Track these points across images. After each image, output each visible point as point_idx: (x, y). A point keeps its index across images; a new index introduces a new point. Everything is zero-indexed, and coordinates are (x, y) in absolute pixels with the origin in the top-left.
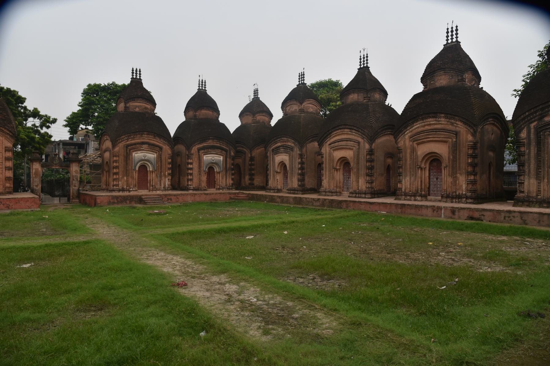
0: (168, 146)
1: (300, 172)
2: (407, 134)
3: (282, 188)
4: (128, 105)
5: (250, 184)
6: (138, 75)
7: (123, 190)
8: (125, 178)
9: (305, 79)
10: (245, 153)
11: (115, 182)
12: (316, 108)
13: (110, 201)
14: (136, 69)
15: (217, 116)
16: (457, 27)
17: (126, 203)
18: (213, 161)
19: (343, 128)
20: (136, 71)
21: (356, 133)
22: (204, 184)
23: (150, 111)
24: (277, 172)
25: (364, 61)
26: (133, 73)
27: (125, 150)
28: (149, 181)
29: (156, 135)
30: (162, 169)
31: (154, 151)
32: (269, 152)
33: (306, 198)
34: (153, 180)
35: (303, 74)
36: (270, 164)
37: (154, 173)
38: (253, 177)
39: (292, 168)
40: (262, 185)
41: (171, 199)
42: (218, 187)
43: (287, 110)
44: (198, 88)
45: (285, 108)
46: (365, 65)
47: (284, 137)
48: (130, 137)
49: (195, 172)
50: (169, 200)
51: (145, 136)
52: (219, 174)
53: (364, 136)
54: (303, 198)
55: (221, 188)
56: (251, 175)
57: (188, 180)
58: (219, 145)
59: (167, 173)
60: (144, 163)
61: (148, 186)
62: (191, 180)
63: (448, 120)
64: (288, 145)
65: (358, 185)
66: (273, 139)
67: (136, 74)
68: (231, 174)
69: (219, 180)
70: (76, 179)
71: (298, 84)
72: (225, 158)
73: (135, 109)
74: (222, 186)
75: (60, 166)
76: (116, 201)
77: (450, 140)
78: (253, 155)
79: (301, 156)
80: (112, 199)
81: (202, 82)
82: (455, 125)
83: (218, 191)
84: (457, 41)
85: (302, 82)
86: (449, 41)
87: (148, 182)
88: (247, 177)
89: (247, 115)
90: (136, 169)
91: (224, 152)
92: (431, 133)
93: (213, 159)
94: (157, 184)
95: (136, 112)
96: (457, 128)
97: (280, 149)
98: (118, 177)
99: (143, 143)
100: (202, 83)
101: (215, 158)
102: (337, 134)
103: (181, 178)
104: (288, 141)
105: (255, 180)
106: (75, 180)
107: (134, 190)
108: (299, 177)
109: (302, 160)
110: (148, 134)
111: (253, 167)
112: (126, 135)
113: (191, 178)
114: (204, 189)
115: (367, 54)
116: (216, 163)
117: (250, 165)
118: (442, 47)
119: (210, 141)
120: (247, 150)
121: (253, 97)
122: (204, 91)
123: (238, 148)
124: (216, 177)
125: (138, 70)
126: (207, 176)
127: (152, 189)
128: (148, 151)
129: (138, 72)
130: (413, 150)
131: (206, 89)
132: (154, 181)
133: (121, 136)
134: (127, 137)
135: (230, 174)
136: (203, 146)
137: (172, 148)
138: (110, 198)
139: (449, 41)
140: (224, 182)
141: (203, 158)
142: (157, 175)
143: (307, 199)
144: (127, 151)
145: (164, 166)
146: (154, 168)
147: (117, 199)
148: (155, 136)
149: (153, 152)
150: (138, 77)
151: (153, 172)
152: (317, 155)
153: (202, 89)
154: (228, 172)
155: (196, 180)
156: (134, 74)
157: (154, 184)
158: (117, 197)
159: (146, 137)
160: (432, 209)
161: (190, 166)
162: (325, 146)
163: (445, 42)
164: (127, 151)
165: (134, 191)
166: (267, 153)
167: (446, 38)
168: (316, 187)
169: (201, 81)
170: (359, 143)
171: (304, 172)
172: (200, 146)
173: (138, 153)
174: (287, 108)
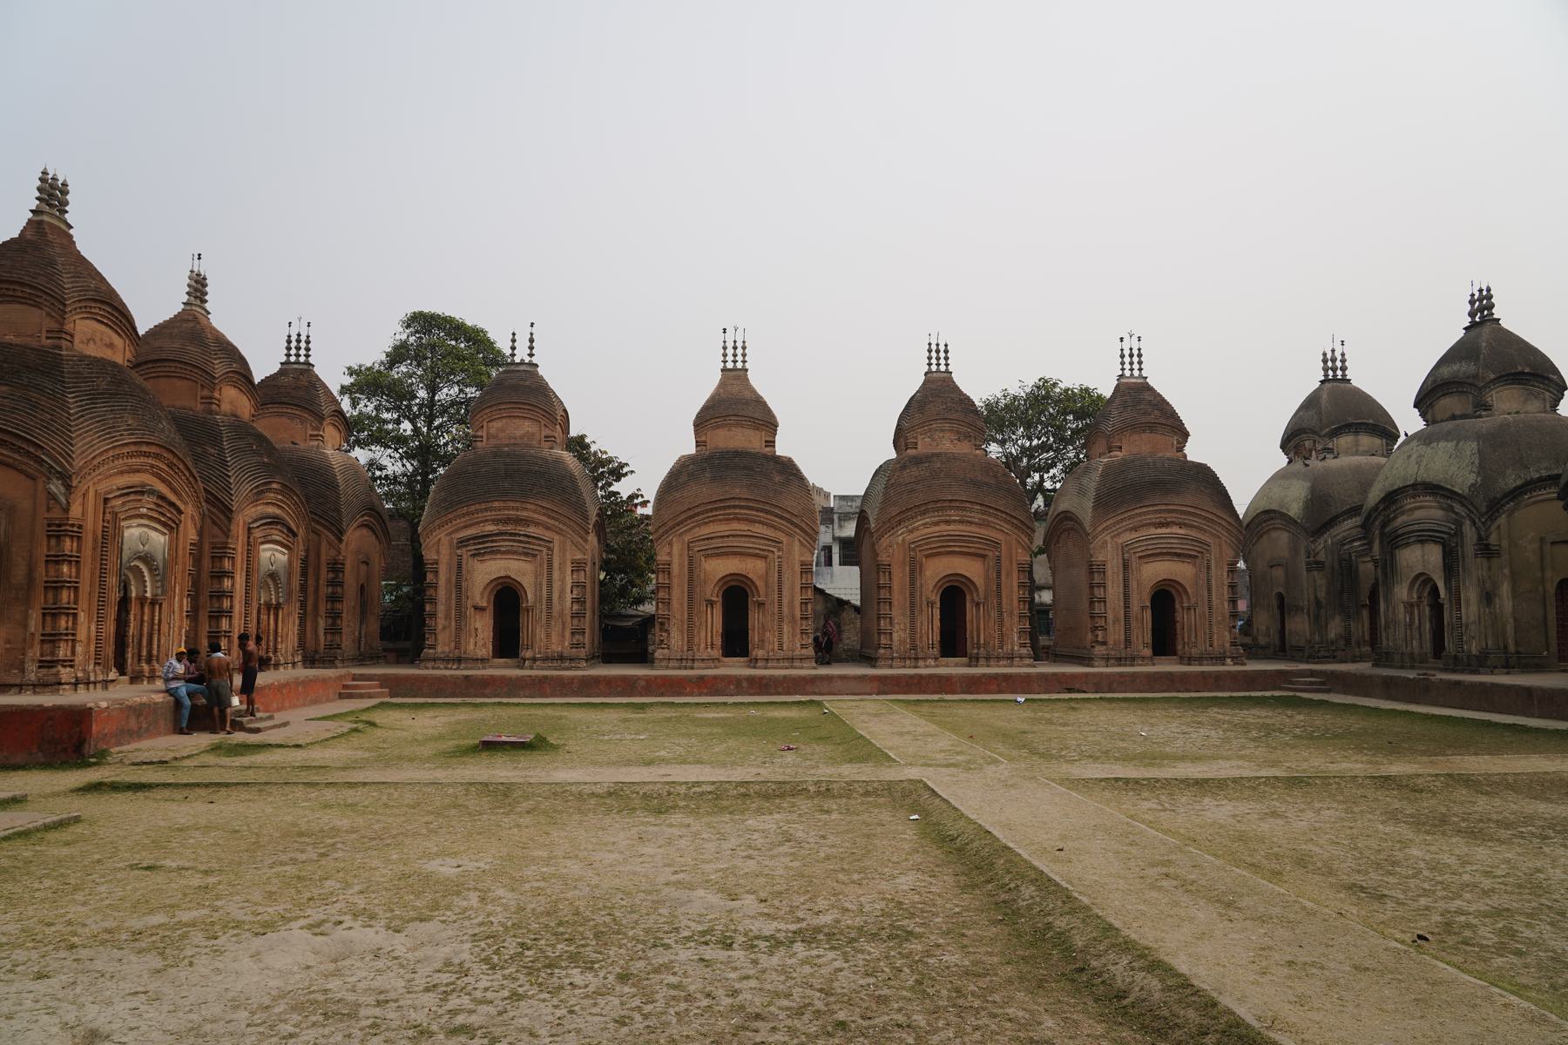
16: (946, 345)
46: (739, 365)
84: (947, 372)
115: (744, 342)
130: (915, 570)
139: (934, 368)
167: (927, 361)
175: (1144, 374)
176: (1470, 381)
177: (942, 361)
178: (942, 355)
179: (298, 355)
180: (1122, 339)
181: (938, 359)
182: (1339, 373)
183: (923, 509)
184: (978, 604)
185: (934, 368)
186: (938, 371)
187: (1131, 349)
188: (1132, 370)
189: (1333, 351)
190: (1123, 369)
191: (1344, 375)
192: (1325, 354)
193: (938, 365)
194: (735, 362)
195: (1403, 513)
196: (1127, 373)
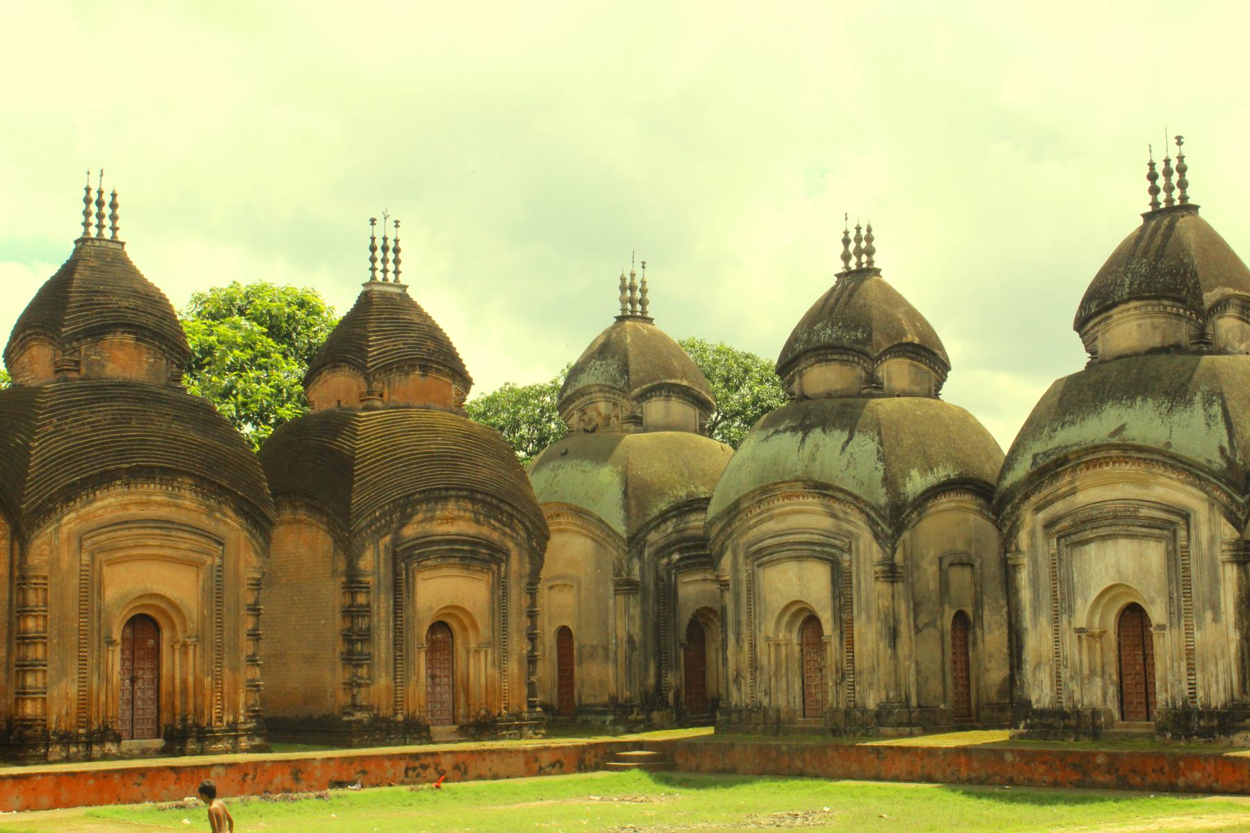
2: (68, 523)
16: (114, 195)
77: (209, 560)
82: (218, 515)
84: (114, 240)
167: (83, 219)
175: (403, 280)
176: (858, 347)
177: (107, 222)
178: (107, 210)
179: (100, 226)
180: (373, 221)
181: (100, 216)
182: (639, 307)
183: (103, 480)
184: (185, 646)
185: (93, 232)
186: (100, 237)
187: (385, 239)
188: (385, 271)
189: (633, 275)
190: (373, 269)
191: (644, 311)
192: (623, 279)
193: (100, 226)
195: (771, 518)
196: (379, 276)
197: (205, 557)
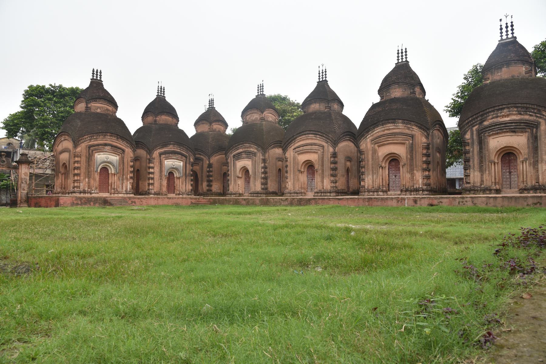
0: (130, 149)
1: (263, 176)
2: (368, 138)
3: (244, 192)
4: (89, 105)
5: (208, 190)
6: (99, 76)
7: (84, 192)
8: (87, 180)
9: (264, 90)
10: (202, 160)
11: (75, 183)
12: (274, 117)
13: (73, 203)
14: (97, 70)
15: (176, 122)
16: (406, 49)
17: (90, 205)
18: (174, 166)
19: (308, 134)
20: (97, 72)
21: (320, 138)
22: (164, 189)
23: (111, 113)
24: (238, 177)
25: (323, 76)
26: (93, 74)
27: (88, 151)
28: (110, 184)
29: (119, 137)
30: (124, 172)
31: (116, 153)
32: (229, 158)
33: (273, 199)
34: (114, 183)
35: (262, 85)
36: (231, 170)
37: (116, 176)
38: (211, 183)
39: (255, 174)
40: (219, 191)
41: (135, 202)
42: (178, 192)
43: (248, 119)
44: (157, 94)
45: (245, 117)
46: (324, 79)
47: (246, 143)
48: (93, 138)
49: (156, 176)
50: (133, 203)
51: (108, 137)
52: (179, 180)
53: (328, 140)
54: (270, 199)
55: (181, 193)
56: (209, 181)
57: (149, 184)
58: (179, 151)
59: (129, 176)
60: (106, 165)
61: (110, 189)
62: (152, 184)
63: (405, 125)
64: (251, 151)
65: (323, 185)
66: (234, 146)
67: (97, 75)
68: (190, 179)
69: (179, 185)
70: (25, 182)
71: (257, 95)
72: (185, 164)
73: (97, 109)
74: (182, 191)
75: (8, 168)
76: (79, 203)
77: (407, 142)
78: (211, 162)
79: (264, 161)
80: (75, 200)
81: (161, 89)
82: (411, 129)
83: (178, 196)
84: (406, 61)
85: (261, 93)
86: (400, 61)
87: (109, 185)
88: (205, 184)
89: (203, 124)
90: (98, 171)
91: (184, 158)
92: (391, 136)
93: (174, 164)
94: (119, 188)
95: (98, 113)
96: (413, 132)
97: (242, 155)
98: (79, 178)
99: (106, 145)
100: (161, 90)
101: (176, 163)
102: (302, 139)
103: (140, 182)
104: (250, 147)
105: (213, 186)
106: (24, 182)
107: (96, 192)
108: (262, 180)
109: (265, 165)
110: (111, 136)
111: (211, 174)
112: (89, 136)
113: (153, 182)
114: (165, 194)
115: (326, 69)
116: (176, 169)
117: (209, 172)
118: (394, 66)
119: (171, 146)
120: (205, 157)
121: (208, 107)
122: (163, 97)
123: (197, 156)
124: (176, 183)
125: (99, 71)
126: (167, 182)
127: (114, 192)
128: (111, 152)
129: (99, 74)
130: (375, 152)
131: (165, 95)
132: (116, 184)
133: (84, 136)
134: (89, 137)
135: (189, 180)
136: (164, 151)
137: (134, 151)
138: (74, 199)
139: (400, 61)
140: (184, 188)
141: (164, 162)
142: (119, 178)
143: (275, 200)
144: (89, 151)
145: (126, 169)
146: (116, 170)
147: (80, 200)
148: (118, 138)
149: (116, 154)
150: (99, 79)
151: (114, 175)
152: (278, 161)
153: (161, 95)
154: (188, 178)
155: (157, 184)
156: (95, 75)
157: (116, 187)
158: (80, 199)
159: (109, 139)
160: (397, 200)
161: (151, 170)
162: (289, 150)
163: (396, 62)
164: (89, 151)
165: (95, 193)
166: (227, 159)
167: (397, 58)
168: (277, 191)
169: (160, 87)
170: (323, 146)
171: (267, 176)
172: (162, 151)
173: (100, 154)
174: (247, 117)
180: (501, 20)
194: (323, 78)
197: (406, 141)
